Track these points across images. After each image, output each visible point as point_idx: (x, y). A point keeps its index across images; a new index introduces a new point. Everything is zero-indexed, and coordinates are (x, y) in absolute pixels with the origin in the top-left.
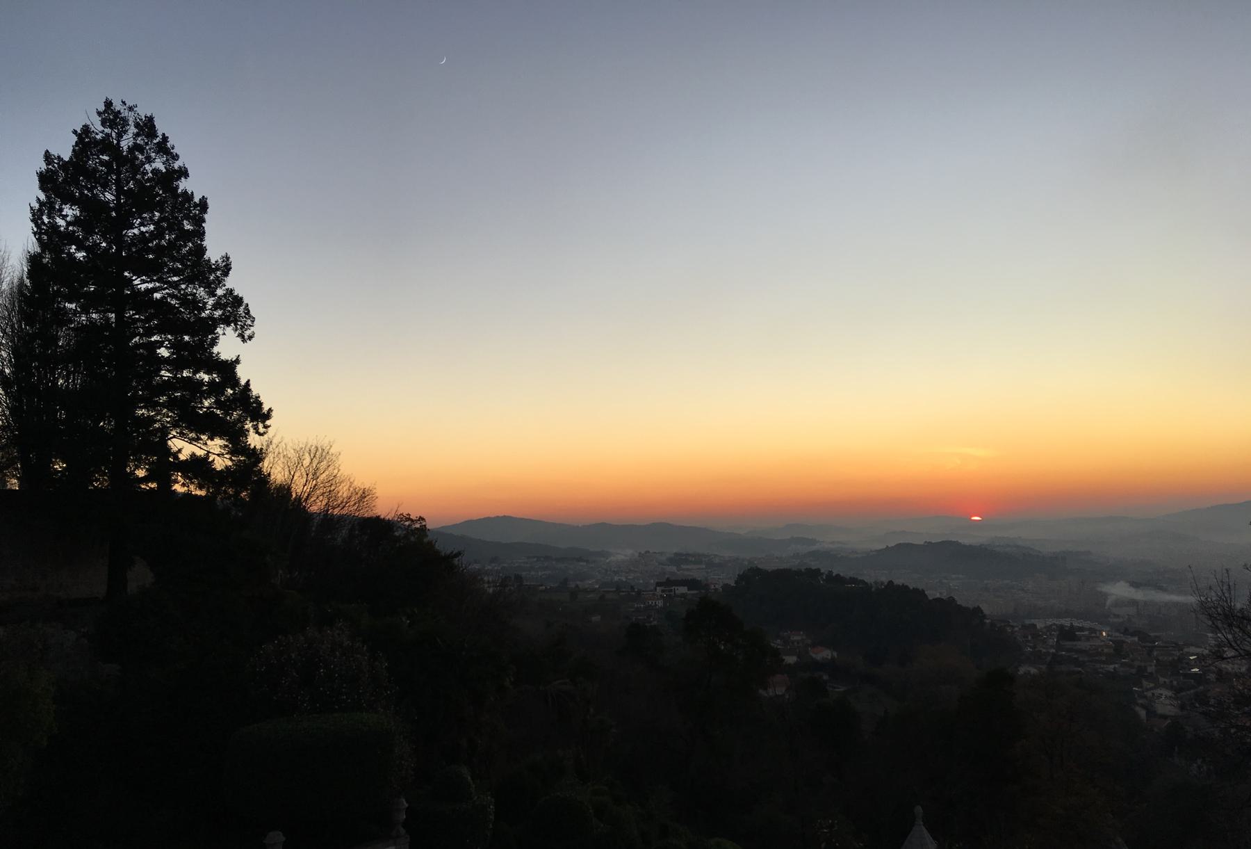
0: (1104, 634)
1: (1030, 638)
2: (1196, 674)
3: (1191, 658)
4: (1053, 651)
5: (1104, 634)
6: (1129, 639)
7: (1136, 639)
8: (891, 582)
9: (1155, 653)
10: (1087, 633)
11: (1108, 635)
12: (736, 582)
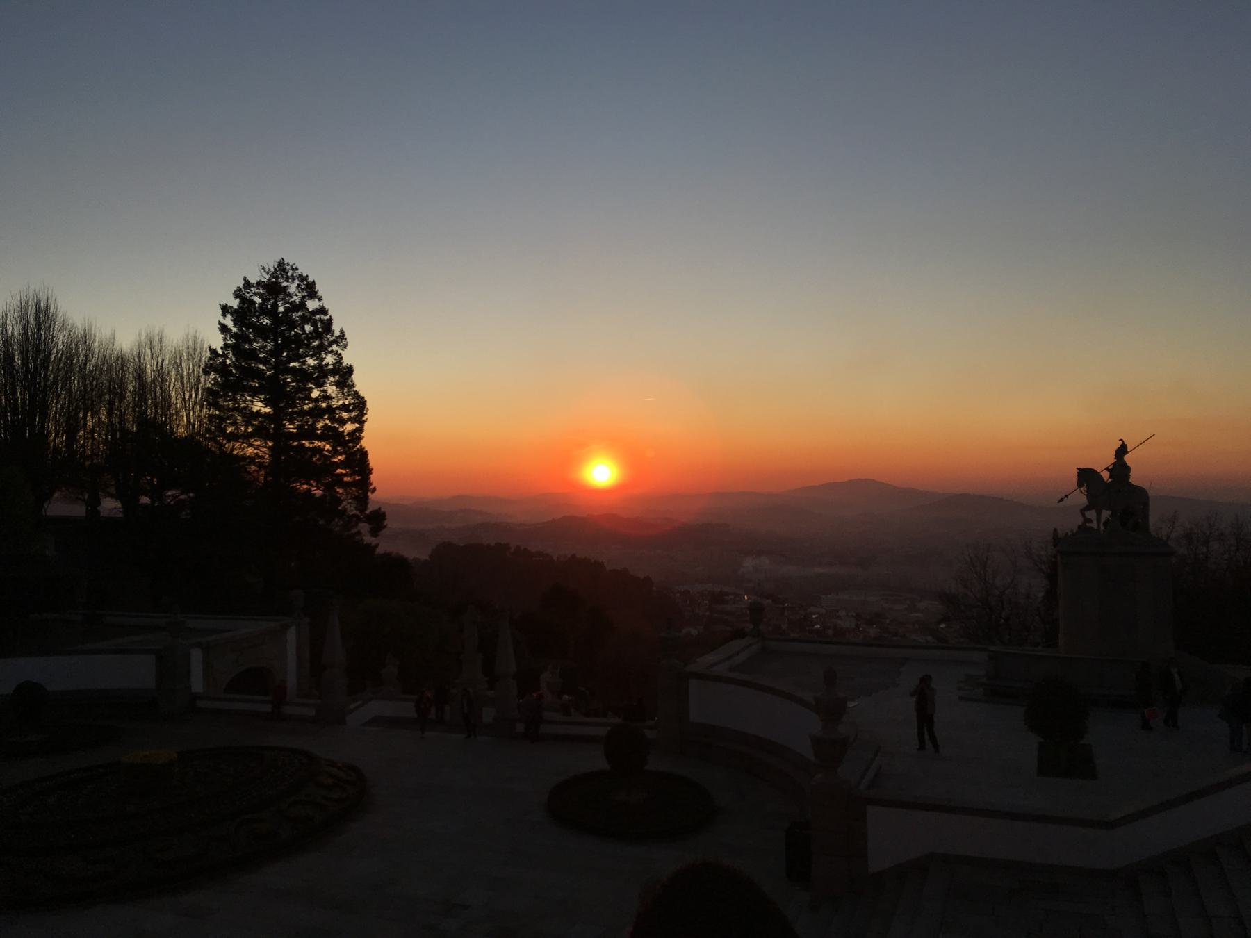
0: (746, 598)
1: (688, 602)
2: (817, 629)
3: (814, 616)
4: (708, 613)
5: (746, 598)
6: (766, 602)
7: (770, 601)
8: (574, 556)
9: (786, 613)
10: (733, 597)
11: (748, 599)
12: (431, 556)
